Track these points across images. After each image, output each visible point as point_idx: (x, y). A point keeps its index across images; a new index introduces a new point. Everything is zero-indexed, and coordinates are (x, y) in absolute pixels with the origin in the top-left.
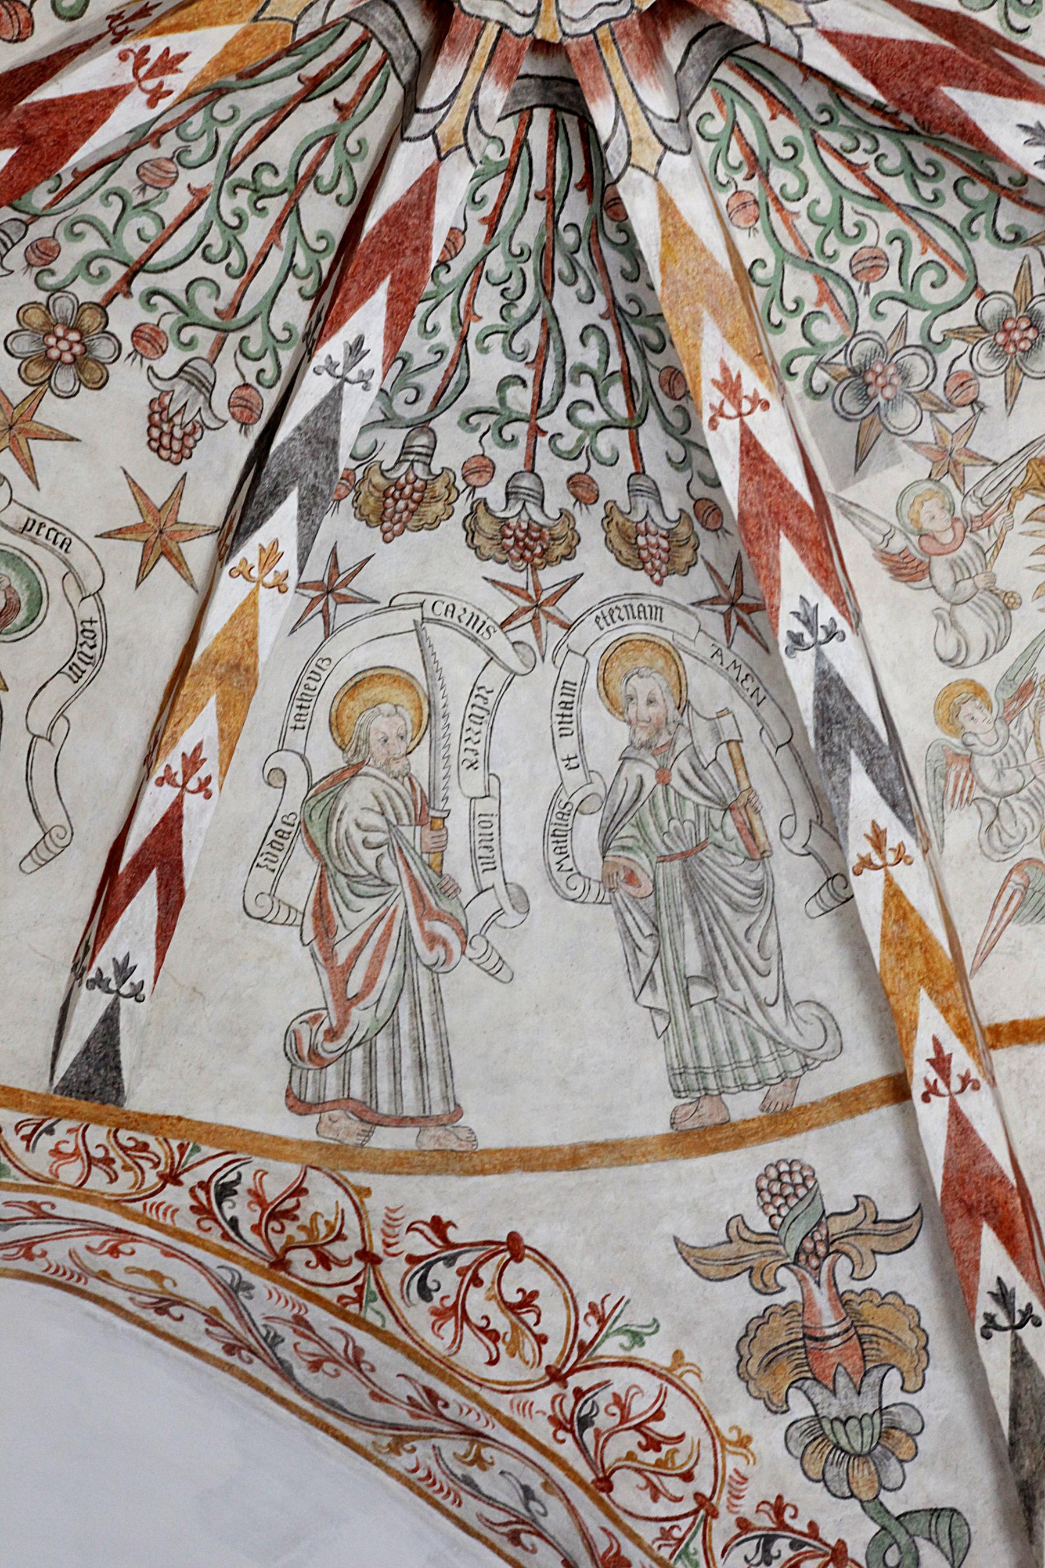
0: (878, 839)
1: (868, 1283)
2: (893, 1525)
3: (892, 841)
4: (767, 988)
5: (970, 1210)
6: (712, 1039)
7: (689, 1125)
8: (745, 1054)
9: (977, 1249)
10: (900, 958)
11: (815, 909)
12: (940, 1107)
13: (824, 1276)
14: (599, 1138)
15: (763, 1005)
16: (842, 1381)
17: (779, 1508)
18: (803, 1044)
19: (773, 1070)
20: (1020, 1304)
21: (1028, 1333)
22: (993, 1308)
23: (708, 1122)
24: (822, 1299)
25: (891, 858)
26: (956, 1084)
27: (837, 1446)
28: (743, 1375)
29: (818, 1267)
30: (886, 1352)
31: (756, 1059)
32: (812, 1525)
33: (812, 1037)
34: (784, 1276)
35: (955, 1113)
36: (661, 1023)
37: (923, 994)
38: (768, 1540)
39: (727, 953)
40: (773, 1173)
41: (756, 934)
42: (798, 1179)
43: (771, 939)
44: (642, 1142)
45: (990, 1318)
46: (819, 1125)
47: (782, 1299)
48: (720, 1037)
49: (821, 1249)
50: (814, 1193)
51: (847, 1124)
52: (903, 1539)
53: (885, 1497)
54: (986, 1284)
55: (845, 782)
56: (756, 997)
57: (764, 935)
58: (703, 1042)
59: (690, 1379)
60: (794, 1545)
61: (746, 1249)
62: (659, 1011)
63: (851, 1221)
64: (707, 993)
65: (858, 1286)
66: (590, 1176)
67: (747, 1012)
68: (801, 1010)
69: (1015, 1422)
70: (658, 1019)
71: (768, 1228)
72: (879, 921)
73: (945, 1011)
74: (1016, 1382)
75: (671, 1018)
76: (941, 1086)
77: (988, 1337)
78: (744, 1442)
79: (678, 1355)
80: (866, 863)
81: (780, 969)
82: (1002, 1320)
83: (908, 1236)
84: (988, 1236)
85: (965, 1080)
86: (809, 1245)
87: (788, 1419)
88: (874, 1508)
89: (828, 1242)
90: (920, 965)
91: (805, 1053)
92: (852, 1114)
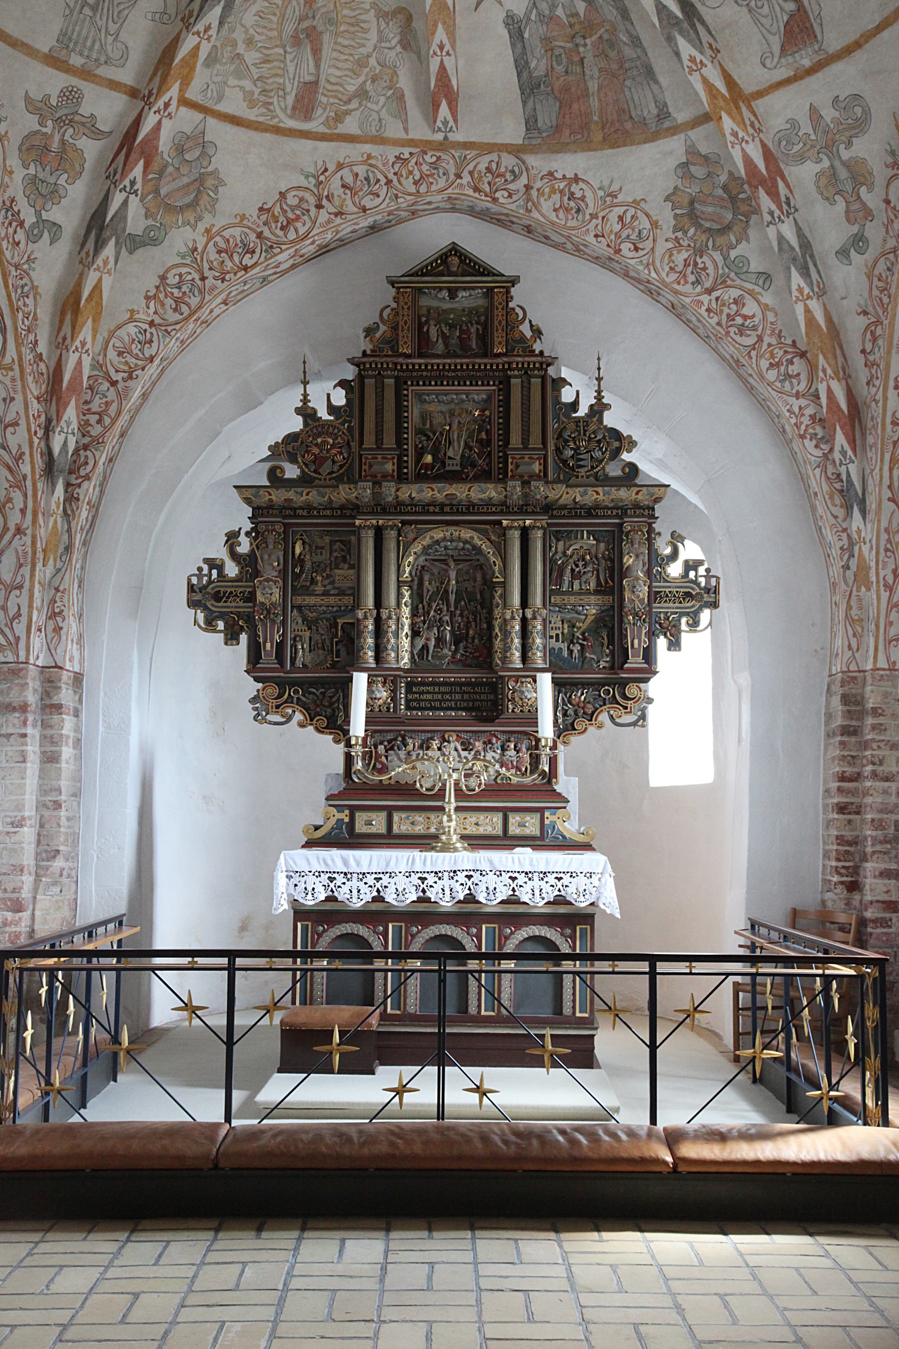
0: (208, 28)
1: (76, 142)
2: (40, 221)
3: (210, 33)
4: (113, 28)
5: (142, 153)
6: (81, 30)
7: (55, 55)
8: (89, 44)
9: (136, 165)
10: (182, 67)
11: (149, 16)
12: (158, 117)
13: (62, 130)
14: (25, 41)
15: (107, 32)
16: (48, 168)
17: (13, 201)
18: (111, 55)
19: (94, 56)
20: (135, 188)
21: (132, 197)
22: (128, 185)
23: (61, 57)
24: (57, 137)
25: (206, 37)
26: (166, 114)
27: (37, 189)
28: (20, 150)
29: (62, 127)
30: (67, 167)
31: (91, 49)
32: (19, 211)
33: (116, 55)
34: (49, 123)
35: (160, 122)
36: (67, 12)
37: (179, 82)
38: (7, 211)
39: (106, 5)
40: (70, 89)
41: (122, 7)
42: (77, 96)
43: (126, 12)
44: (38, 51)
45: (125, 186)
46: (97, 84)
47: (44, 130)
48: (84, 32)
49: (67, 122)
50: (79, 104)
51: (107, 90)
52: (41, 227)
53: (43, 212)
54: (131, 176)
55: (214, 6)
56: (107, 28)
57: (124, 9)
58: (77, 29)
59: (6, 142)
60: (13, 215)
61: (45, 108)
62: (69, 6)
63: (84, 120)
64: (89, 13)
65: (71, 141)
66: (17, 53)
67: (100, 31)
68: (119, 44)
69: (112, 220)
70: (67, 9)
71: (55, 104)
72: (186, 52)
73: (180, 90)
74: (120, 208)
75: (72, 11)
76: (162, 112)
77: (120, 191)
78: (11, 172)
79: (7, 132)
80: (198, 33)
81: (121, 25)
82: (128, 189)
83: (101, 137)
84: (142, 162)
85: (169, 114)
86: (64, 118)
87: (27, 172)
88: (38, 214)
89: (71, 121)
90: (185, 73)
91: (109, 58)
92: (111, 89)
